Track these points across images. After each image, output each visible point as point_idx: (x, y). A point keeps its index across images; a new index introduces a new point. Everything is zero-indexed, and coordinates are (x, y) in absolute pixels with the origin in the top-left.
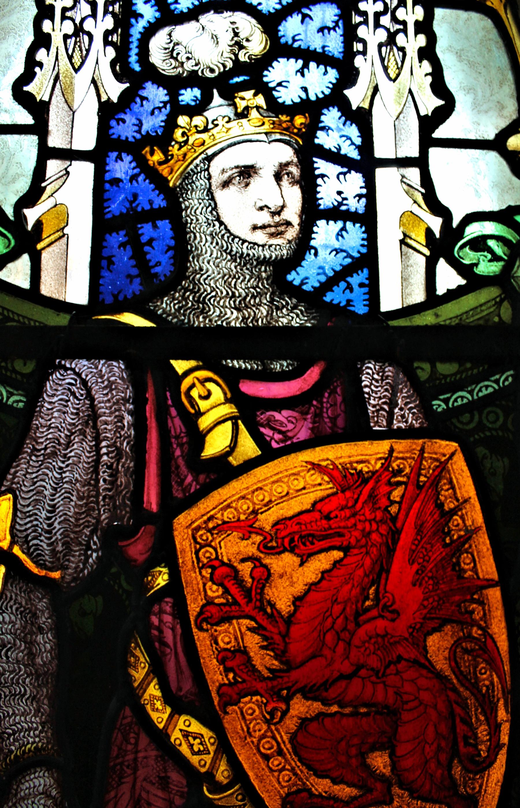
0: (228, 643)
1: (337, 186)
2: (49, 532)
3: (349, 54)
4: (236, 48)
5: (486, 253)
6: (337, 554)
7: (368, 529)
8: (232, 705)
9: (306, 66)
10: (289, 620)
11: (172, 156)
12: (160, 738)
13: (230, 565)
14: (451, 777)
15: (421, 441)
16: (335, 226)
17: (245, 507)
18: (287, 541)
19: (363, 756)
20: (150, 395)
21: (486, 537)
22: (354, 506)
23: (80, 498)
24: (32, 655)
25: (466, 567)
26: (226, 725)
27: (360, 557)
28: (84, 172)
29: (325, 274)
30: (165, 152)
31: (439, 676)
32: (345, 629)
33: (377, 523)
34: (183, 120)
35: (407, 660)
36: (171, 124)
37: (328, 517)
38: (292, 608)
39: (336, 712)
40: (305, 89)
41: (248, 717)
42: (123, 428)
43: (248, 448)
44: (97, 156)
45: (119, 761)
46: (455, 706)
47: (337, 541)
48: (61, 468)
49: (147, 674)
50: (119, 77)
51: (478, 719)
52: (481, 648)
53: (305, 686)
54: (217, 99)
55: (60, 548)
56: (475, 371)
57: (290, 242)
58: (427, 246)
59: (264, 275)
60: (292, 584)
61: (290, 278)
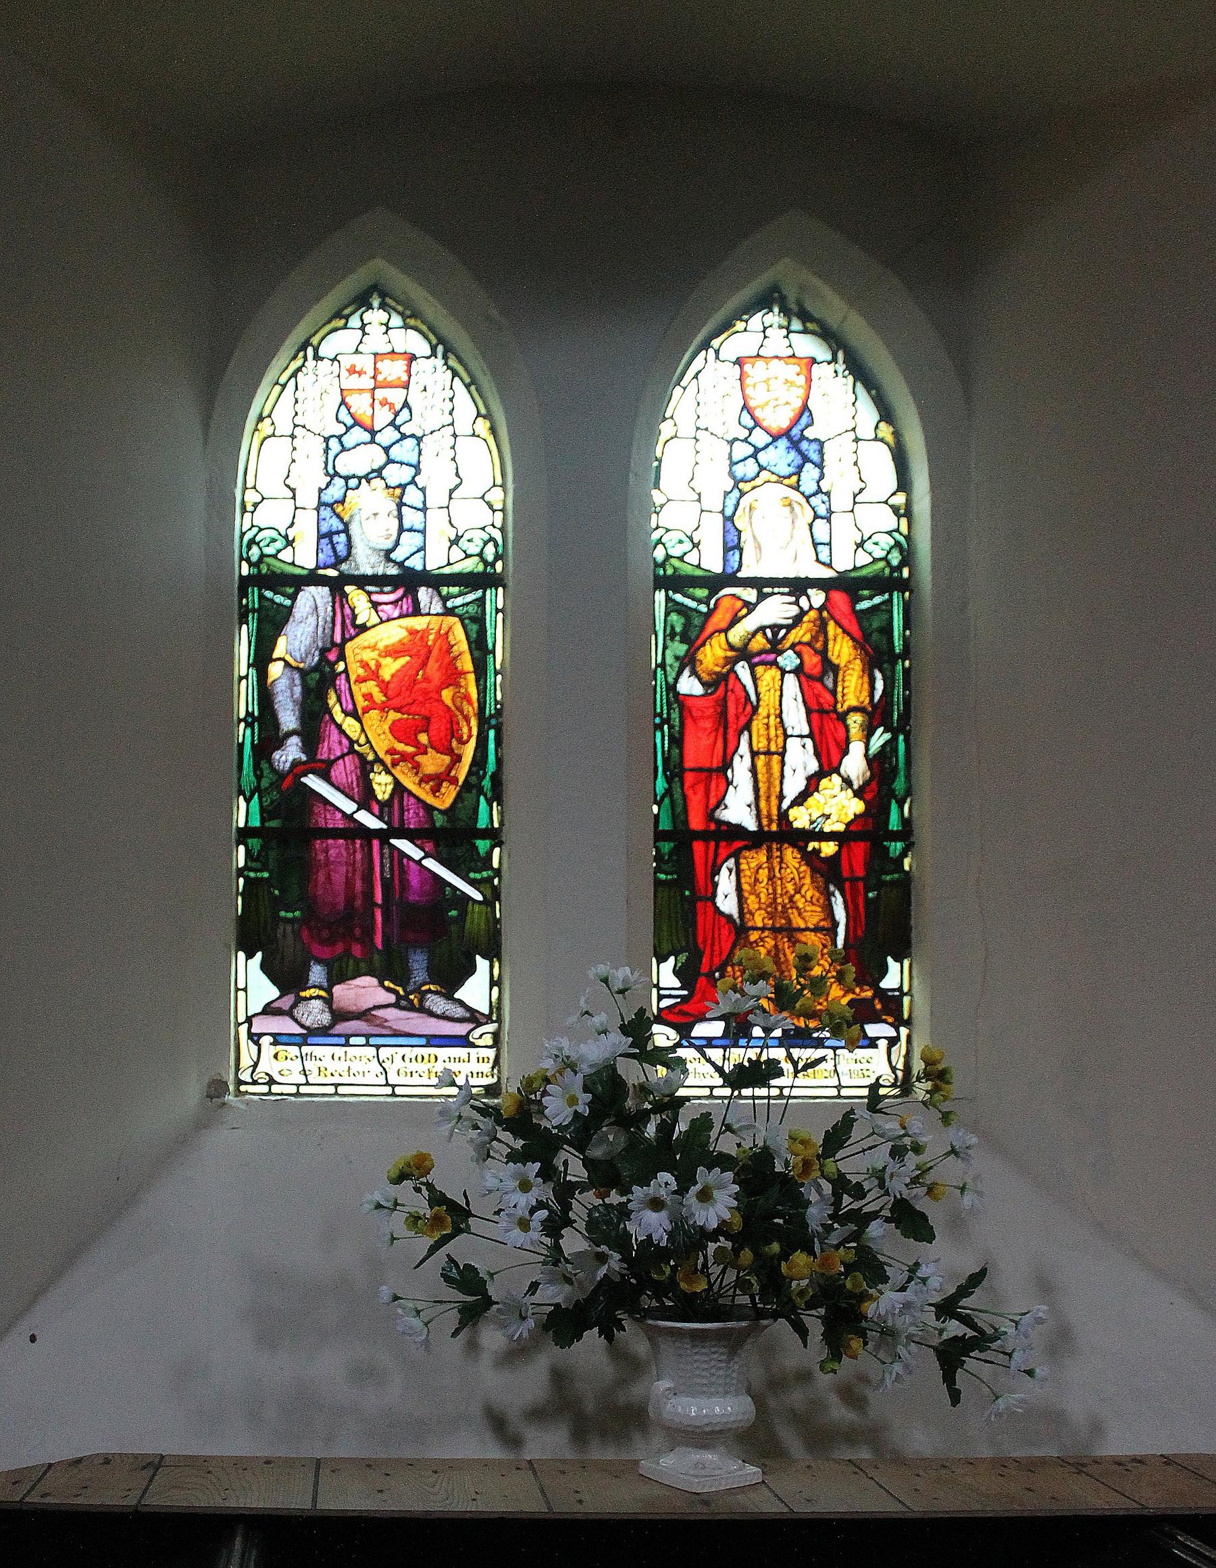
6: (408, 658)
12: (339, 727)
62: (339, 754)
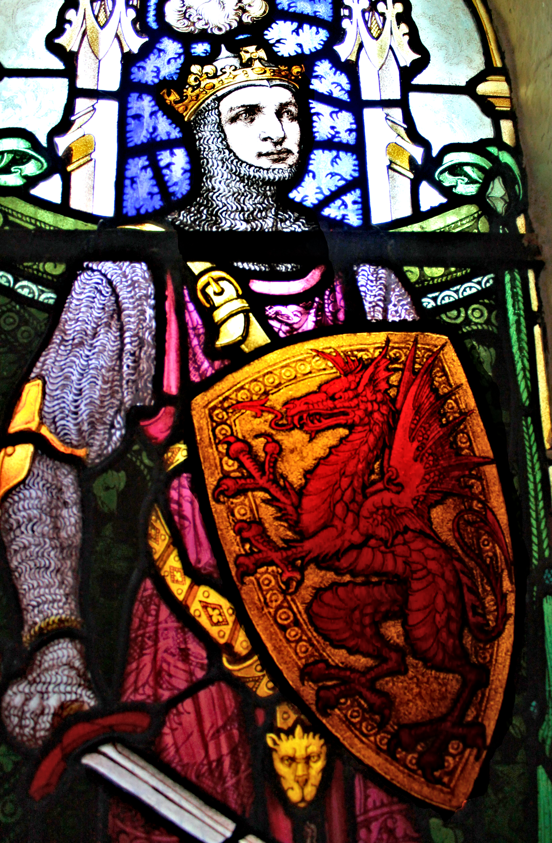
0: (244, 515)
1: (329, 122)
2: (76, 413)
3: (337, 18)
4: (240, 12)
5: (463, 177)
6: (343, 432)
7: (370, 409)
8: (249, 575)
9: (300, 27)
10: (301, 492)
11: (187, 96)
12: (180, 610)
13: (244, 441)
14: (463, 646)
15: (414, 334)
16: (329, 155)
17: (257, 389)
18: (296, 418)
19: (376, 625)
20: (170, 292)
21: (479, 419)
22: (356, 388)
23: (105, 382)
24: (57, 529)
25: (463, 445)
26: (244, 596)
27: (364, 434)
28: (110, 109)
29: (322, 193)
30: (181, 93)
31: (444, 546)
32: (353, 500)
33: (378, 403)
34: (195, 68)
35: (412, 531)
36: (184, 71)
37: (333, 398)
38: (303, 481)
39: (349, 582)
40: (300, 46)
41: (265, 588)
42: (144, 321)
43: (258, 336)
44: (121, 96)
45: (141, 632)
46: (461, 575)
47: (342, 420)
48: (87, 356)
49: (168, 546)
50: (139, 33)
51: (484, 590)
52: (482, 521)
53: (318, 556)
54: (224, 52)
55: (85, 427)
56: (459, 274)
57: (291, 166)
58: (411, 170)
59: (269, 193)
60: (302, 459)
61: (291, 195)
62: (181, 684)
